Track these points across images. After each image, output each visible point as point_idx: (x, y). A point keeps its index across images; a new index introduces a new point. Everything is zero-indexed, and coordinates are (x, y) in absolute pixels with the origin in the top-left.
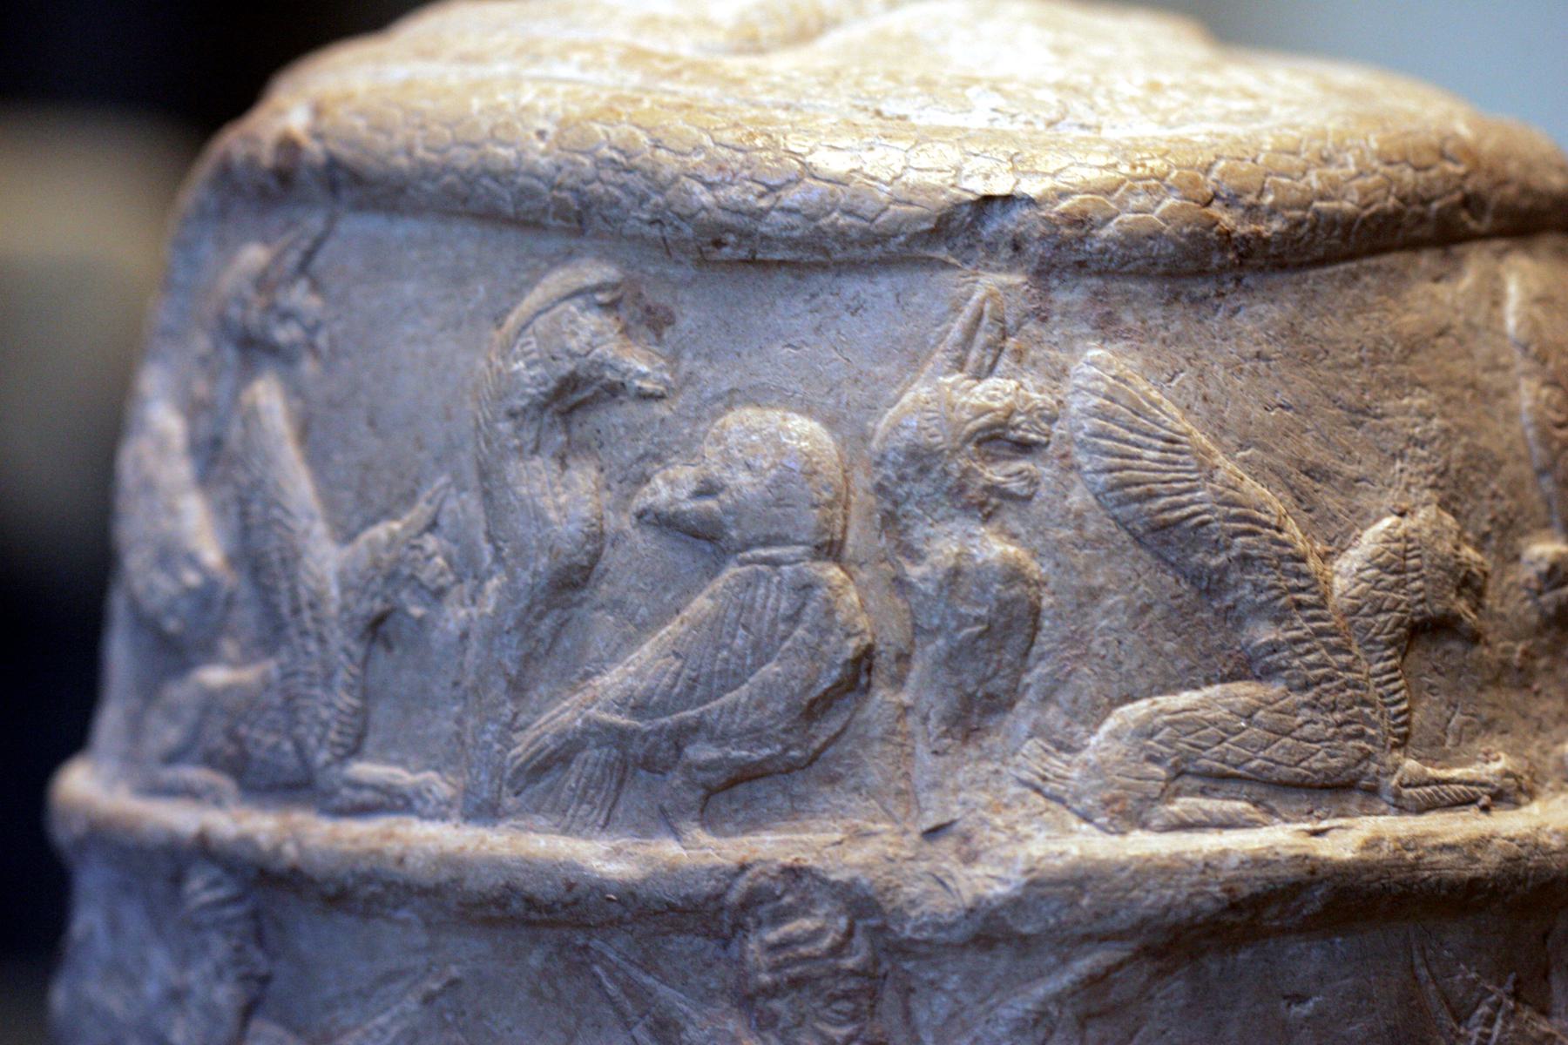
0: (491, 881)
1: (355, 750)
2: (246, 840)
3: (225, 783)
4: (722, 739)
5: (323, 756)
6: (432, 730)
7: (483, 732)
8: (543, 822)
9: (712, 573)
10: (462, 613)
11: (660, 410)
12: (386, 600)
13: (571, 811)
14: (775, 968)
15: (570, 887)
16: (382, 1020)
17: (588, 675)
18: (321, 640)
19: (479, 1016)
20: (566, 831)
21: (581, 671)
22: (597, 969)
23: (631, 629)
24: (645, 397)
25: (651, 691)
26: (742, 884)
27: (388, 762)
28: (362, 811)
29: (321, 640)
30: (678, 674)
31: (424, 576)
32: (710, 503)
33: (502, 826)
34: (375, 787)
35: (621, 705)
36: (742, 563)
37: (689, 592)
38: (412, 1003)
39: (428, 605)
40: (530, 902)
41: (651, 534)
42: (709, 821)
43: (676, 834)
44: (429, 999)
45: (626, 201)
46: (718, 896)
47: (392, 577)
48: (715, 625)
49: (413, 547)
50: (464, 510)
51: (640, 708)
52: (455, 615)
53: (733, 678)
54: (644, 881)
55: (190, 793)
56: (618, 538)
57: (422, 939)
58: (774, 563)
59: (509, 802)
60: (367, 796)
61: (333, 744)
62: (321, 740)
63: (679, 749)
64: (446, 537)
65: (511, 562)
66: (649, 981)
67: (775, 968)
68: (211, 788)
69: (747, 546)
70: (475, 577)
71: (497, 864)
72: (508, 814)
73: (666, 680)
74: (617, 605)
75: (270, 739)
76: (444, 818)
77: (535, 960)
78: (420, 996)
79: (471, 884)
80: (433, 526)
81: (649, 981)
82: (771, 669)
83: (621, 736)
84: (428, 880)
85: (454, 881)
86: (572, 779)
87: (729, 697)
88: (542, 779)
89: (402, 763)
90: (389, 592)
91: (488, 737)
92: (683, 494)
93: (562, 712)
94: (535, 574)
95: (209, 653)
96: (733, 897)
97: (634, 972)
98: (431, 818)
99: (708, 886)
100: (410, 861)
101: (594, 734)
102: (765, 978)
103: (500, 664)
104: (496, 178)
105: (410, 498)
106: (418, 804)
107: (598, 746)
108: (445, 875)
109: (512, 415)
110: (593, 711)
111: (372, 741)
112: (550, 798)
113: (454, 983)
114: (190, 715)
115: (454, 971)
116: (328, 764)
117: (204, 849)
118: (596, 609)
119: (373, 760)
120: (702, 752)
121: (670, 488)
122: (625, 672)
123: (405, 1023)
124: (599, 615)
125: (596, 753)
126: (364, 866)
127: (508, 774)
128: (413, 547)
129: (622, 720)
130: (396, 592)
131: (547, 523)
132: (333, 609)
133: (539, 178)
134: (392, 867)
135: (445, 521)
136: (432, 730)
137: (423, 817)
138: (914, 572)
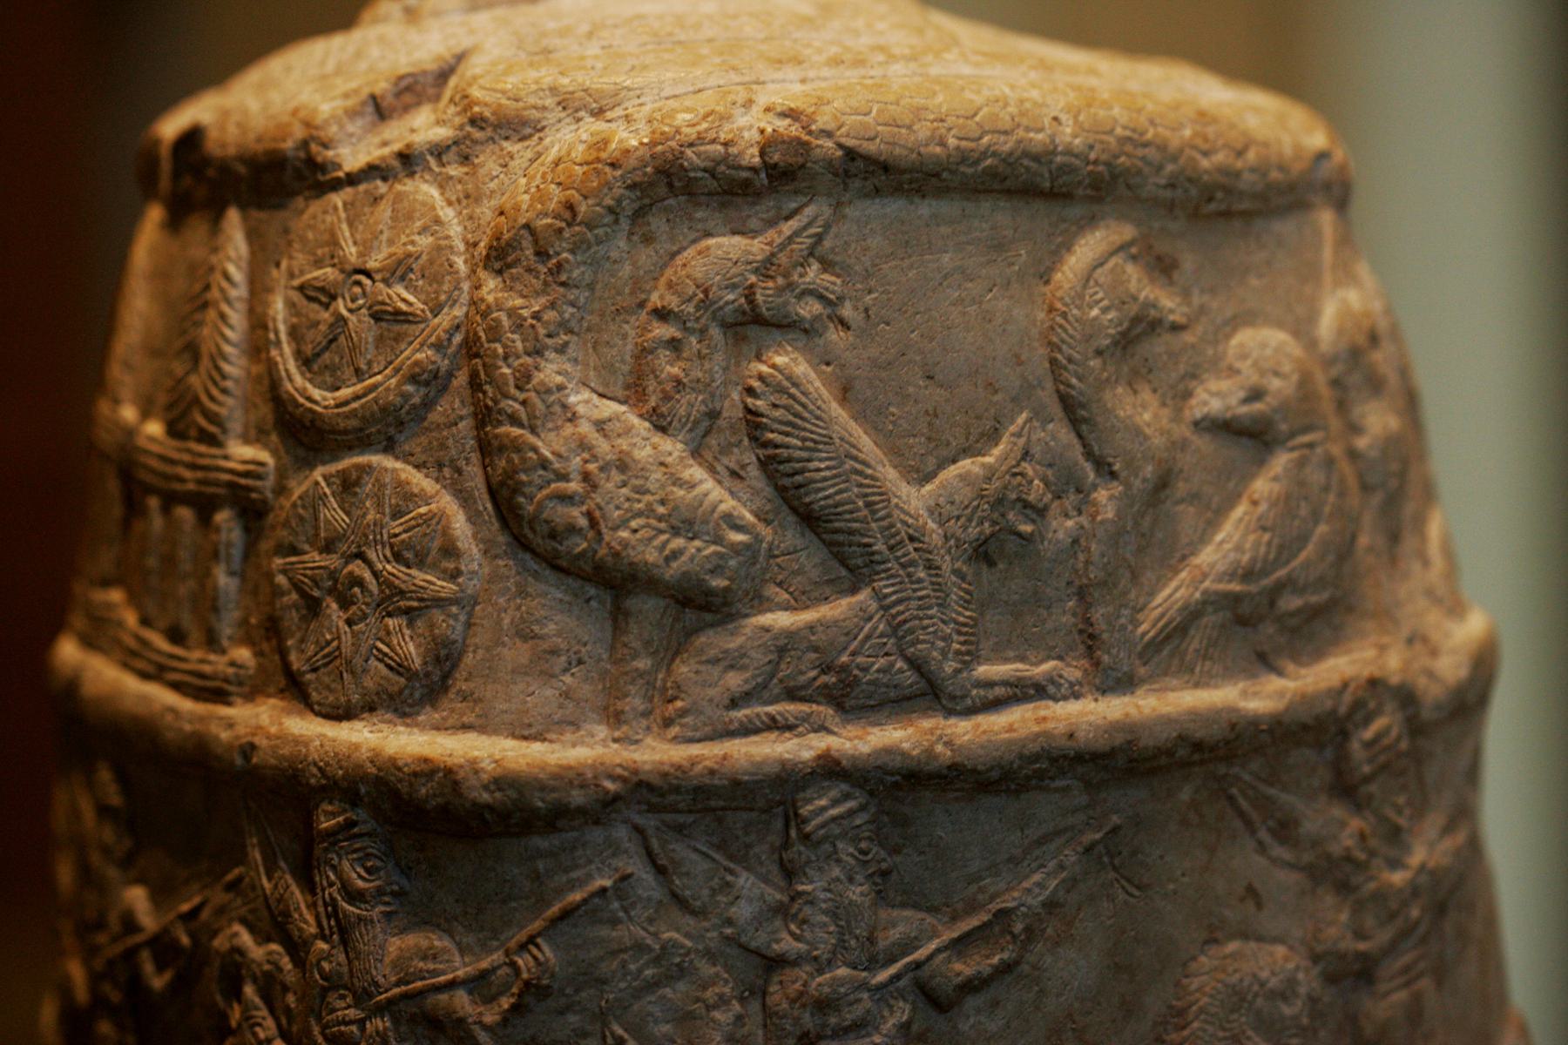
0: (1165, 735)
1: (971, 657)
2: (888, 751)
3: (825, 711)
4: (1300, 590)
5: (950, 666)
6: (1049, 625)
7: (1119, 617)
8: (1175, 682)
9: (1261, 463)
10: (1070, 523)
11: (1188, 337)
12: (994, 523)
13: (1198, 669)
14: (1370, 761)
15: (1233, 726)
16: (1037, 877)
17: (1184, 558)
18: (930, 566)
19: (1134, 853)
20: (1197, 685)
21: (1178, 555)
22: (1234, 791)
23: (1209, 514)
24: (1176, 328)
25: (1254, 560)
26: (1348, 698)
27: (1007, 660)
28: (996, 705)
29: (930, 566)
30: (1269, 544)
31: (1031, 498)
32: (1258, 407)
33: (1140, 692)
34: (1005, 683)
35: (1231, 575)
36: (1292, 449)
37: (1247, 478)
38: (1071, 856)
39: (1033, 521)
40: (1198, 746)
41: (1207, 437)
42: (1296, 658)
43: (1280, 673)
44: (1089, 850)
45: (1146, 170)
46: (1334, 711)
47: (999, 502)
48: (1286, 503)
49: (1015, 475)
50: (1054, 438)
51: (1248, 575)
52: (1062, 527)
53: (1303, 539)
54: (1287, 710)
55: (775, 725)
56: (1183, 445)
57: (1083, 799)
58: (1311, 446)
59: (1142, 671)
60: (999, 691)
61: (958, 653)
62: (944, 653)
63: (1272, 604)
64: (1039, 463)
65: (1124, 474)
66: (1272, 791)
67: (1370, 761)
68: (806, 718)
69: (1293, 435)
70: (1079, 491)
71: (1168, 720)
72: (1143, 681)
73: (1263, 550)
74: (1194, 497)
75: (882, 662)
76: (1077, 696)
77: (1185, 795)
78: (1080, 849)
79: (1147, 741)
80: (1026, 455)
81: (1272, 791)
82: (1322, 528)
83: (1236, 598)
84: (1102, 744)
85: (1129, 742)
86: (1195, 642)
87: (1303, 555)
88: (1171, 650)
89: (1022, 659)
90: (995, 516)
91: (1123, 620)
92: (1233, 401)
93: (1176, 589)
94: (1144, 480)
95: (761, 603)
96: (1343, 710)
97: (1263, 788)
98: (1065, 698)
99: (1329, 704)
100: (1081, 735)
101: (1212, 603)
102: (1367, 769)
103: (1125, 560)
104: (1036, 158)
105: (993, 436)
106: (1051, 689)
107: (1216, 611)
108: (1119, 739)
109: (1099, 353)
110: (1207, 584)
111: (986, 646)
112: (1176, 662)
113: (1115, 830)
114: (759, 658)
115: (1115, 819)
116: (957, 671)
117: (830, 769)
118: (1178, 503)
119: (988, 661)
120: (1291, 602)
121: (1216, 397)
122: (1223, 548)
123: (1064, 874)
124: (1181, 507)
125: (1213, 618)
126: (1034, 748)
127: (1139, 648)
128: (1015, 475)
129: (1235, 587)
130: (1003, 515)
131: (1146, 438)
132: (936, 538)
133: (1076, 156)
134: (1064, 742)
135: (1036, 450)
136: (1049, 625)
137: (1056, 700)
138: (1362, 443)
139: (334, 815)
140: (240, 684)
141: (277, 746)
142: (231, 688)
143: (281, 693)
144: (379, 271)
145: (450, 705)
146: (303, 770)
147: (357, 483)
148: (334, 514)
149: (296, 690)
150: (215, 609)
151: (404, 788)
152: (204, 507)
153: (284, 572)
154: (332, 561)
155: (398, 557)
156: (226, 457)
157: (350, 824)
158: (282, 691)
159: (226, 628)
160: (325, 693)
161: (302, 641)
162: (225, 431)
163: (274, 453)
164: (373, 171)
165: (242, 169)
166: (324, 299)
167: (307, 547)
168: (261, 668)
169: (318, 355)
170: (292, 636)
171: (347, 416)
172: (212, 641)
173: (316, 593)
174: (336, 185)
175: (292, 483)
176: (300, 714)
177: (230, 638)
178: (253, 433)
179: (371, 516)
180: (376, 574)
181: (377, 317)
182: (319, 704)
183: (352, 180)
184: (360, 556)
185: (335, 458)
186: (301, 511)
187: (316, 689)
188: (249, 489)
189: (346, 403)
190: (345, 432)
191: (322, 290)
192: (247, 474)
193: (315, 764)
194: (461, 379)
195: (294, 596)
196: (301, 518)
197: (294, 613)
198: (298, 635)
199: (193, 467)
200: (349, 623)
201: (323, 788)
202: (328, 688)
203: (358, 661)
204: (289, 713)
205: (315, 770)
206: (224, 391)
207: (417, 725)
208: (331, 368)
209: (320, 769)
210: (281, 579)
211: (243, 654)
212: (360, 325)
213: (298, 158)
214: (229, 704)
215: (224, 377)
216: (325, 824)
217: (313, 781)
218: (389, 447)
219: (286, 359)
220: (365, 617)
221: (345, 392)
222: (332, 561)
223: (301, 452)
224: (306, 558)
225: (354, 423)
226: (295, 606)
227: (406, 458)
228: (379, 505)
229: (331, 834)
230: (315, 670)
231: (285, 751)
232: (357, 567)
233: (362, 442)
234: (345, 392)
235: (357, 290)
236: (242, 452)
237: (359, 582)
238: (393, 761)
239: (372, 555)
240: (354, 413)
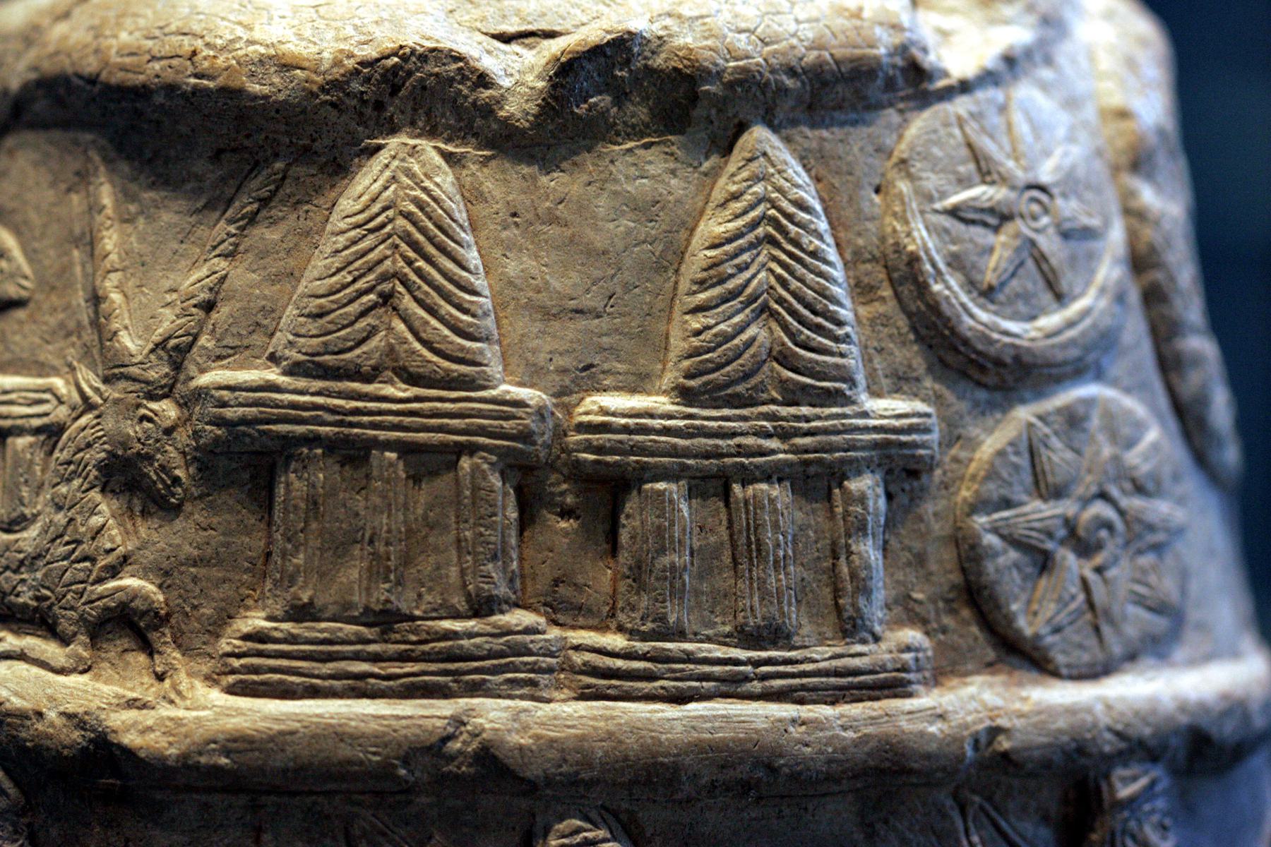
139: (1134, 779)
140: (919, 670)
141: (1043, 722)
142: (911, 676)
143: (989, 667)
144: (1057, 184)
145: (1190, 635)
146: (1094, 739)
147: (1086, 418)
148: (1058, 456)
149: (1021, 655)
150: (867, 592)
151: (1214, 731)
152: (817, 479)
153: (995, 530)
154: (1066, 507)
155: (1139, 489)
156: (865, 415)
157: (1153, 784)
158: (990, 665)
159: (876, 612)
160: (1077, 653)
161: (1029, 602)
162: (853, 383)
163: (938, 400)
164: (988, 78)
165: (789, 82)
166: (992, 221)
167: (1024, 498)
168: (940, 647)
169: (1003, 284)
170: (1016, 599)
171: (1064, 346)
172: (851, 627)
173: (1049, 545)
174: (948, 94)
175: (974, 431)
176: (1036, 683)
177: (881, 622)
178: (885, 382)
179: (1107, 451)
180: (1121, 512)
181: (1066, 235)
182: (1068, 666)
183: (965, 87)
184: (1103, 496)
185: (1040, 394)
186: (1014, 459)
187: (1064, 652)
188: (914, 445)
189: (1057, 332)
190: (1065, 363)
191: (991, 211)
192: (911, 429)
193: (1110, 729)
194: (1134, 297)
195: (1013, 555)
196: (1016, 467)
197: (1015, 573)
198: (1024, 597)
199: (784, 435)
200: (1099, 570)
201: (1120, 753)
202: (1081, 646)
203: (1116, 609)
204: (1020, 684)
205: (1108, 736)
206: (846, 339)
207: (1173, 665)
208: (1025, 297)
209: (1118, 734)
210: (991, 539)
211: (912, 635)
212: (1049, 243)
213: (894, 66)
214: (910, 695)
215: (840, 323)
216: (1124, 792)
217: (1107, 749)
218: (1099, 375)
219: (949, 288)
220: (1116, 560)
221: (1050, 321)
222: (1066, 507)
223: (982, 395)
224: (1026, 509)
225: (1074, 353)
226: (1016, 565)
227: (1114, 383)
228: (1113, 436)
229: (1132, 801)
230: (1057, 630)
231: (1061, 723)
232: (1100, 509)
233: (1077, 370)
234: (1050, 321)
235: (1035, 208)
236: (888, 408)
237: (1109, 526)
238: (1203, 707)
239: (1114, 492)
240: (1072, 342)
